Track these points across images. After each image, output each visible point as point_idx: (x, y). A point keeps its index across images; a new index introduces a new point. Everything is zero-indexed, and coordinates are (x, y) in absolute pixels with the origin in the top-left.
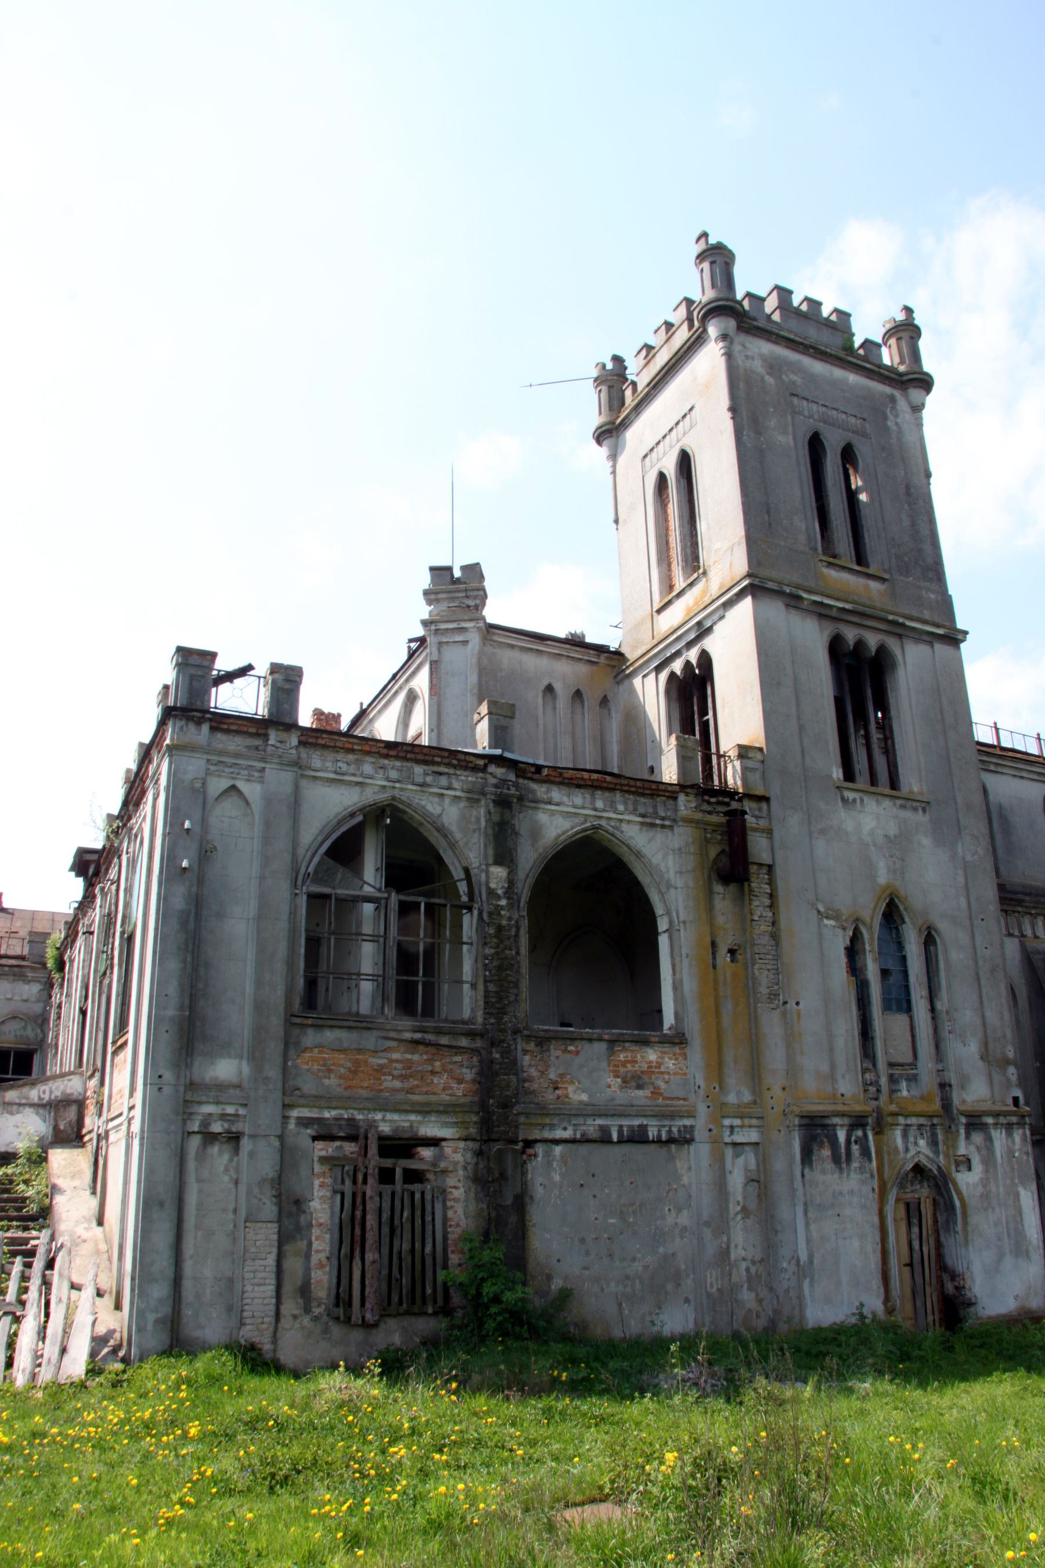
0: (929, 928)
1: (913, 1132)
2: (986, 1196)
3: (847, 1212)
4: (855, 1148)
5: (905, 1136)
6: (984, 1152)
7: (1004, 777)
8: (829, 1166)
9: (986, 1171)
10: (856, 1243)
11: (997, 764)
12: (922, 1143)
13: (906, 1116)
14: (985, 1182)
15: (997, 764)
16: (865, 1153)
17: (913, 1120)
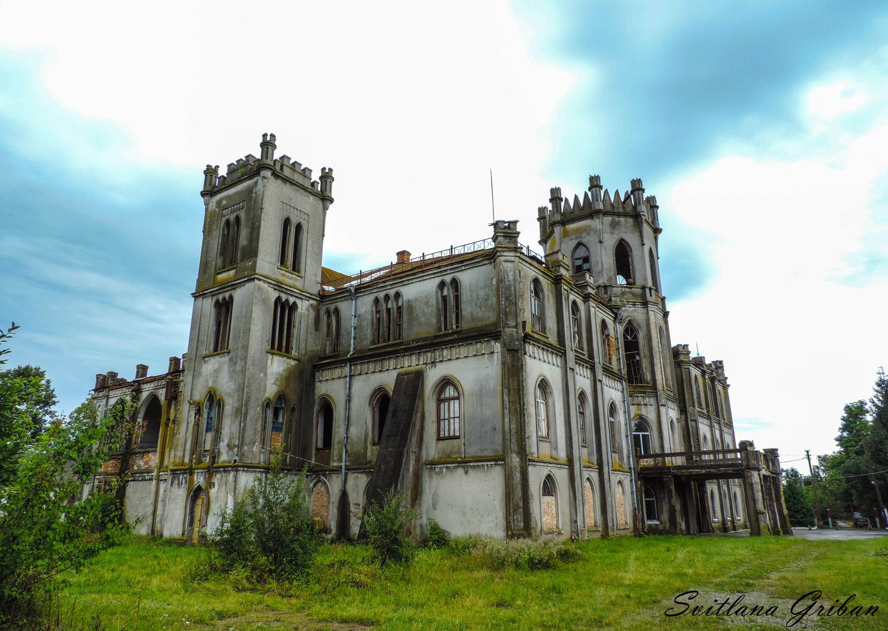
0: (219, 400)
1: (200, 474)
2: (217, 498)
3: (178, 501)
4: (184, 480)
5: (197, 476)
6: (219, 481)
7: (415, 284)
8: (177, 486)
9: (219, 488)
10: (178, 511)
11: (408, 280)
12: (202, 478)
13: (197, 469)
14: (218, 492)
15: (408, 280)
16: (186, 482)
17: (199, 471)
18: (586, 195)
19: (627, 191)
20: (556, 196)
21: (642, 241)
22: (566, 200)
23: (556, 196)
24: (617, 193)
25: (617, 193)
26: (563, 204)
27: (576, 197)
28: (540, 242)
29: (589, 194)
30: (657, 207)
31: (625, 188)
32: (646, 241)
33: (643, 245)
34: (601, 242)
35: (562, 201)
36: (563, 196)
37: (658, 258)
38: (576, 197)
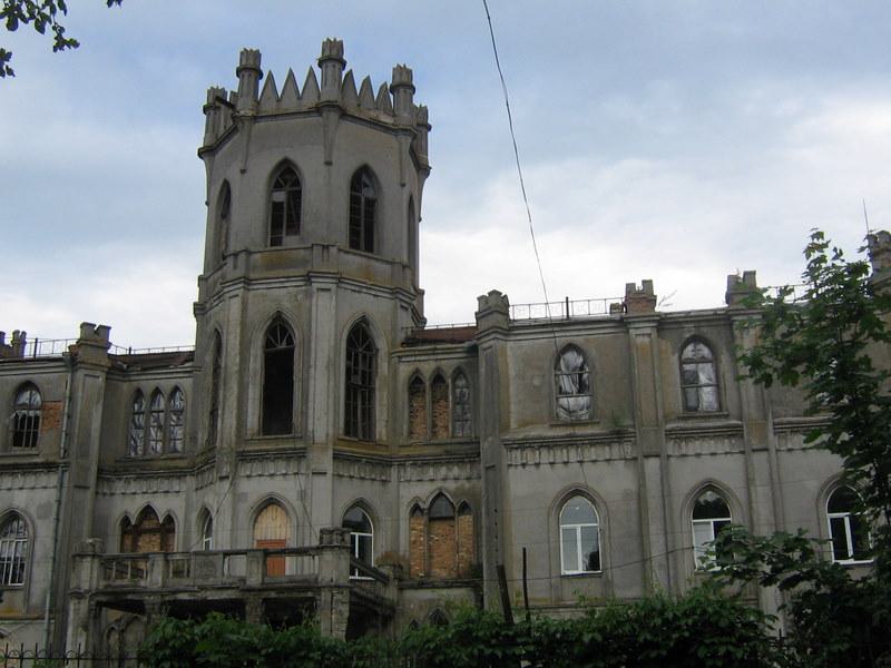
18: (311, 73)
19: (386, 83)
20: (250, 67)
21: (402, 177)
22: (271, 76)
23: (250, 67)
24: (367, 82)
25: (367, 82)
26: (262, 83)
27: (291, 75)
28: (201, 154)
29: (318, 72)
30: (429, 128)
31: (382, 77)
32: (407, 180)
33: (403, 185)
34: (329, 163)
35: (261, 77)
36: (265, 68)
37: (420, 220)
38: (291, 75)
